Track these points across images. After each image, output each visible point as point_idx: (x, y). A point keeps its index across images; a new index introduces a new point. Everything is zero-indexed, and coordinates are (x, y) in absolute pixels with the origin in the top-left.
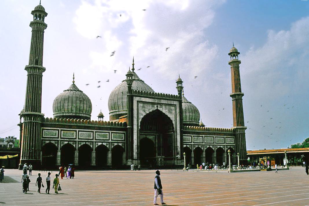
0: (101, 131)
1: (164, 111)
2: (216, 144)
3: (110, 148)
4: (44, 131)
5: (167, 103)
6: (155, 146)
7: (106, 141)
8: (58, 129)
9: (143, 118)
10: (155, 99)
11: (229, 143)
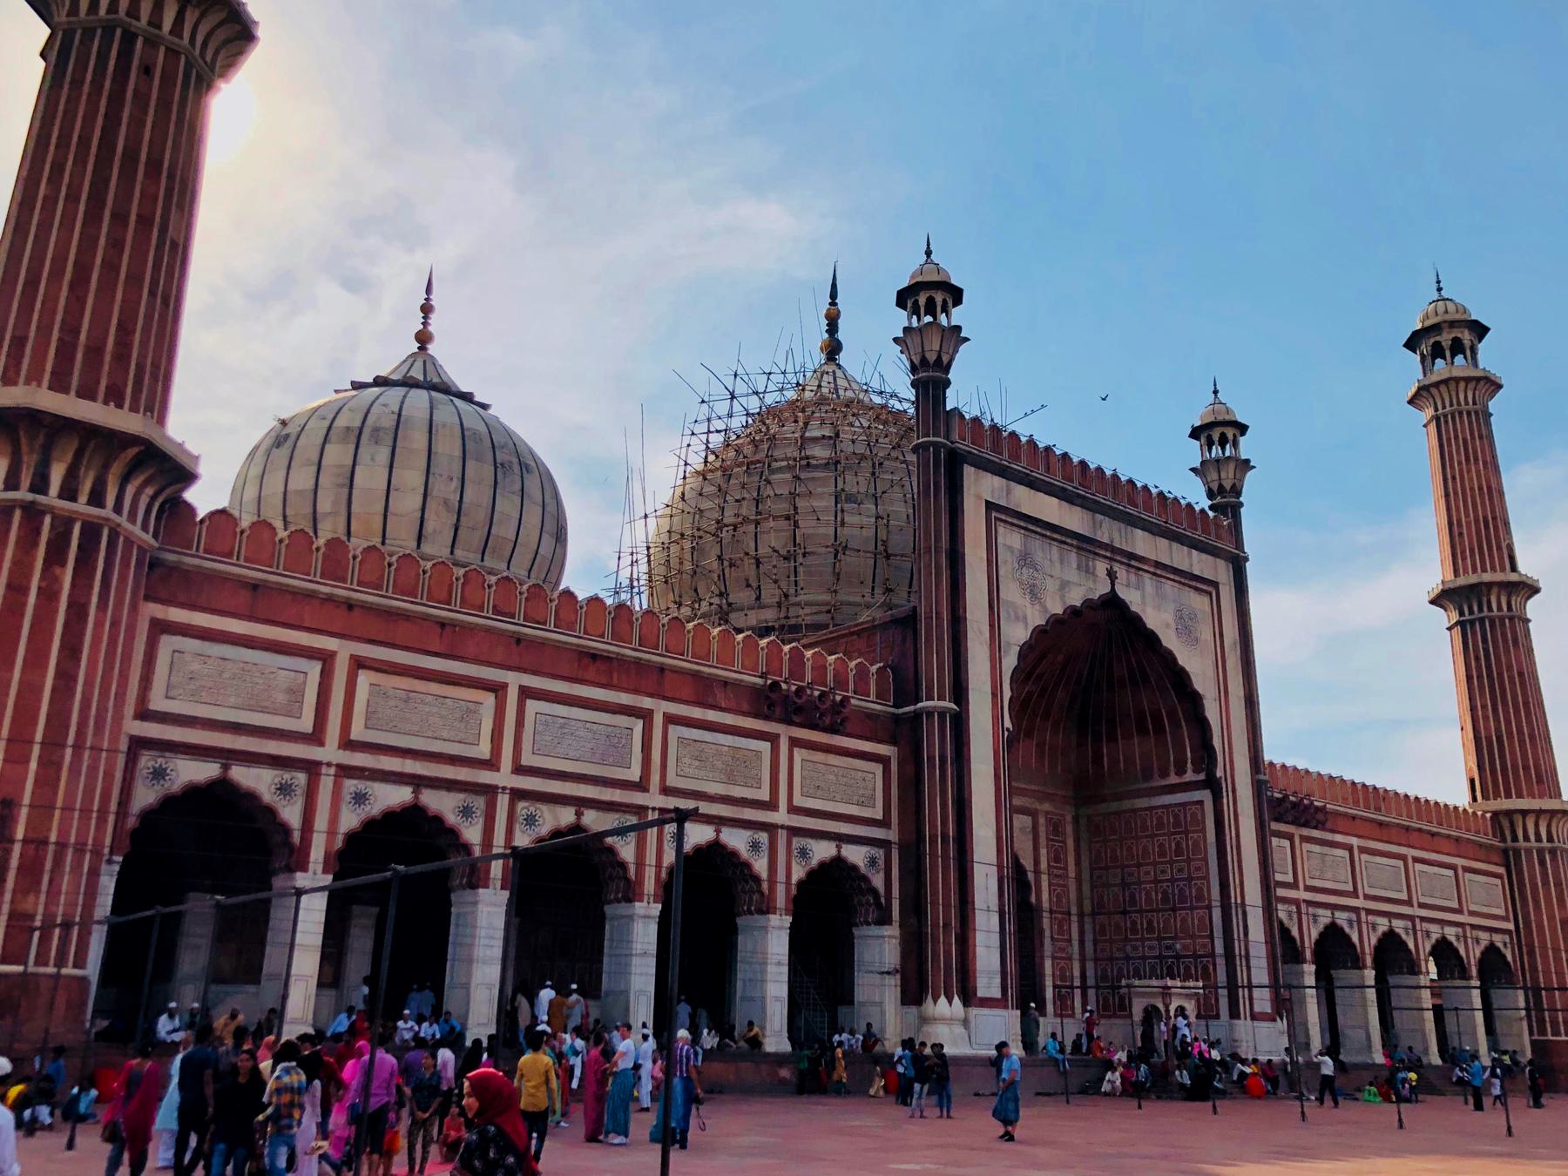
0: (712, 716)
2: (1424, 913)
4: (167, 643)
6: (1033, 899)
9: (1026, 651)
10: (1099, 517)
11: (1485, 910)
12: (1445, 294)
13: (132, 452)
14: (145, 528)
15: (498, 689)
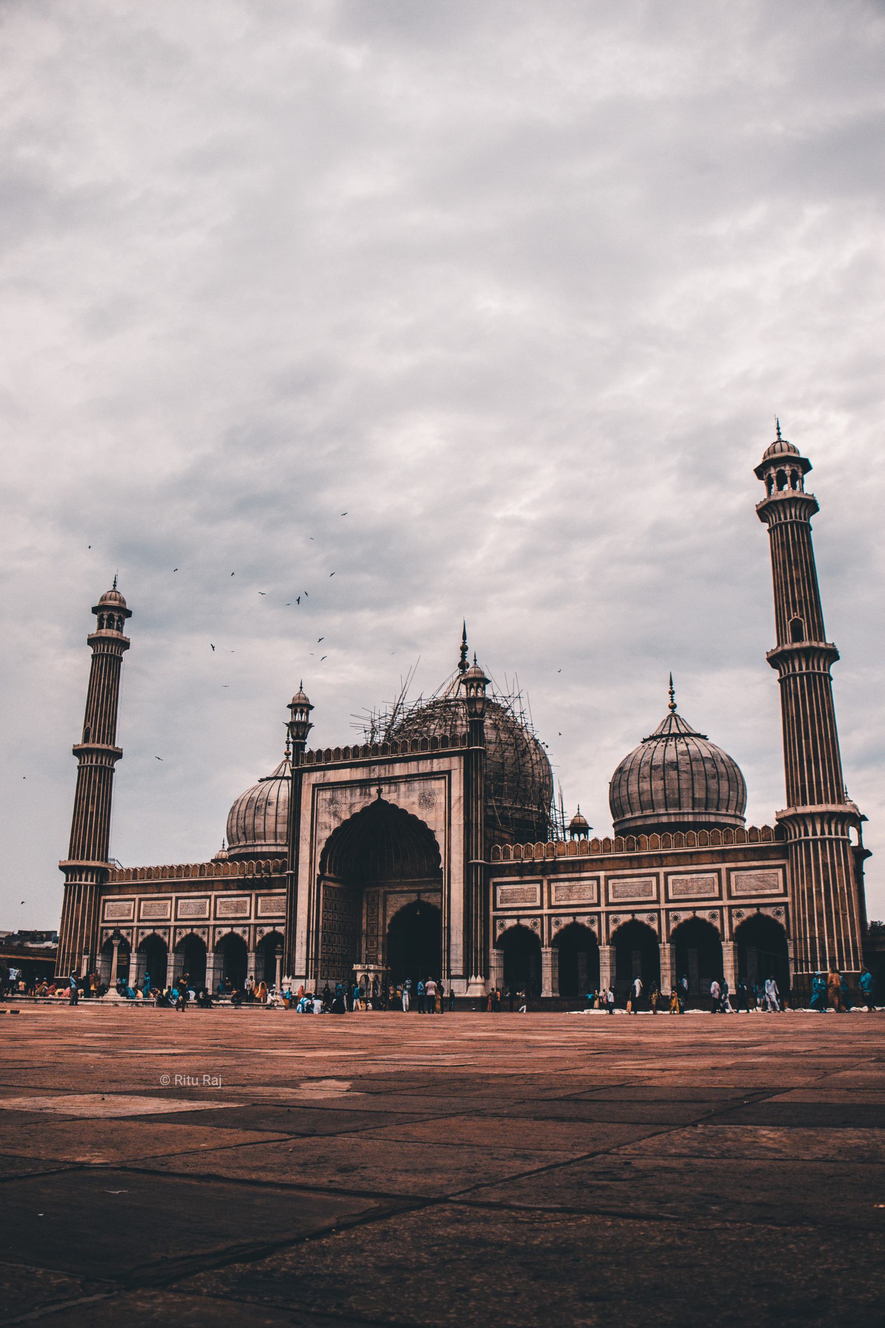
0: (229, 893)
1: (402, 804)
3: (252, 939)
4: (107, 904)
5: (416, 772)
7: (241, 922)
8: (134, 896)
9: (329, 841)
11: (754, 893)
12: (783, 437)
13: (76, 868)
14: (92, 881)
15: (170, 898)
